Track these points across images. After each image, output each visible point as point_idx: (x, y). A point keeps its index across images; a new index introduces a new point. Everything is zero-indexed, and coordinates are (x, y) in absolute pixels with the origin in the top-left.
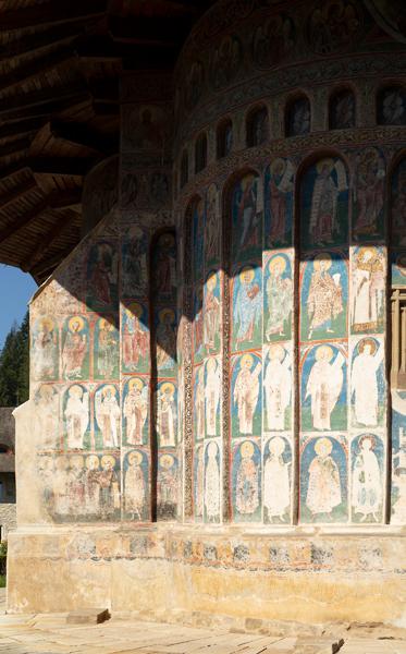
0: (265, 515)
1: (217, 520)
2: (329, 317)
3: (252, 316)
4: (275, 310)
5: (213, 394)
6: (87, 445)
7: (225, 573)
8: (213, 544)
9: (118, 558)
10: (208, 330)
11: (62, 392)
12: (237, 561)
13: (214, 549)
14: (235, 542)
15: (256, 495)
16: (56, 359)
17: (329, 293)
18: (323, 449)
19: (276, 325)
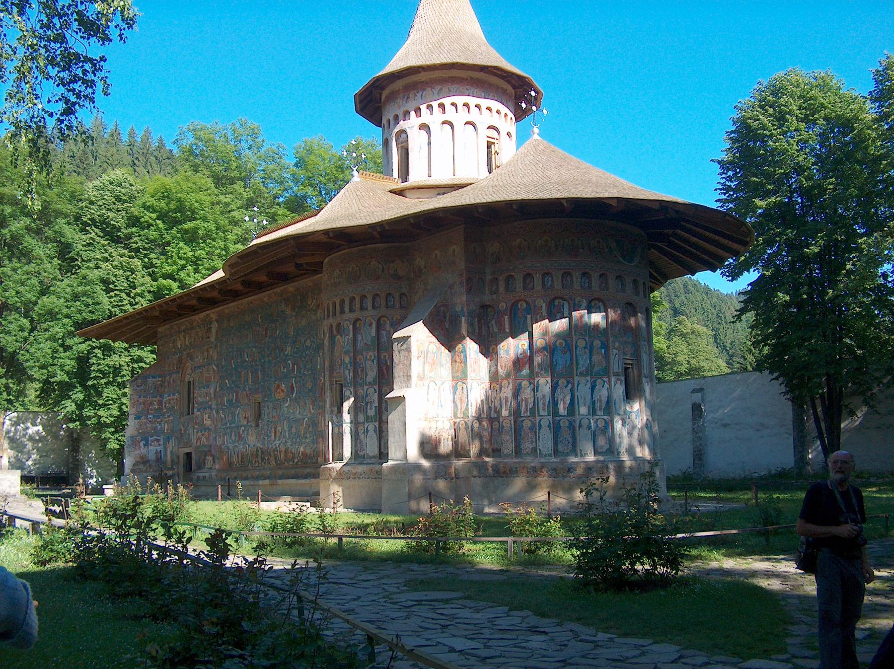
0: (581, 453)
1: (550, 455)
4: (581, 362)
9: (475, 477)
11: (426, 385)
15: (570, 444)
16: (423, 367)
19: (582, 369)
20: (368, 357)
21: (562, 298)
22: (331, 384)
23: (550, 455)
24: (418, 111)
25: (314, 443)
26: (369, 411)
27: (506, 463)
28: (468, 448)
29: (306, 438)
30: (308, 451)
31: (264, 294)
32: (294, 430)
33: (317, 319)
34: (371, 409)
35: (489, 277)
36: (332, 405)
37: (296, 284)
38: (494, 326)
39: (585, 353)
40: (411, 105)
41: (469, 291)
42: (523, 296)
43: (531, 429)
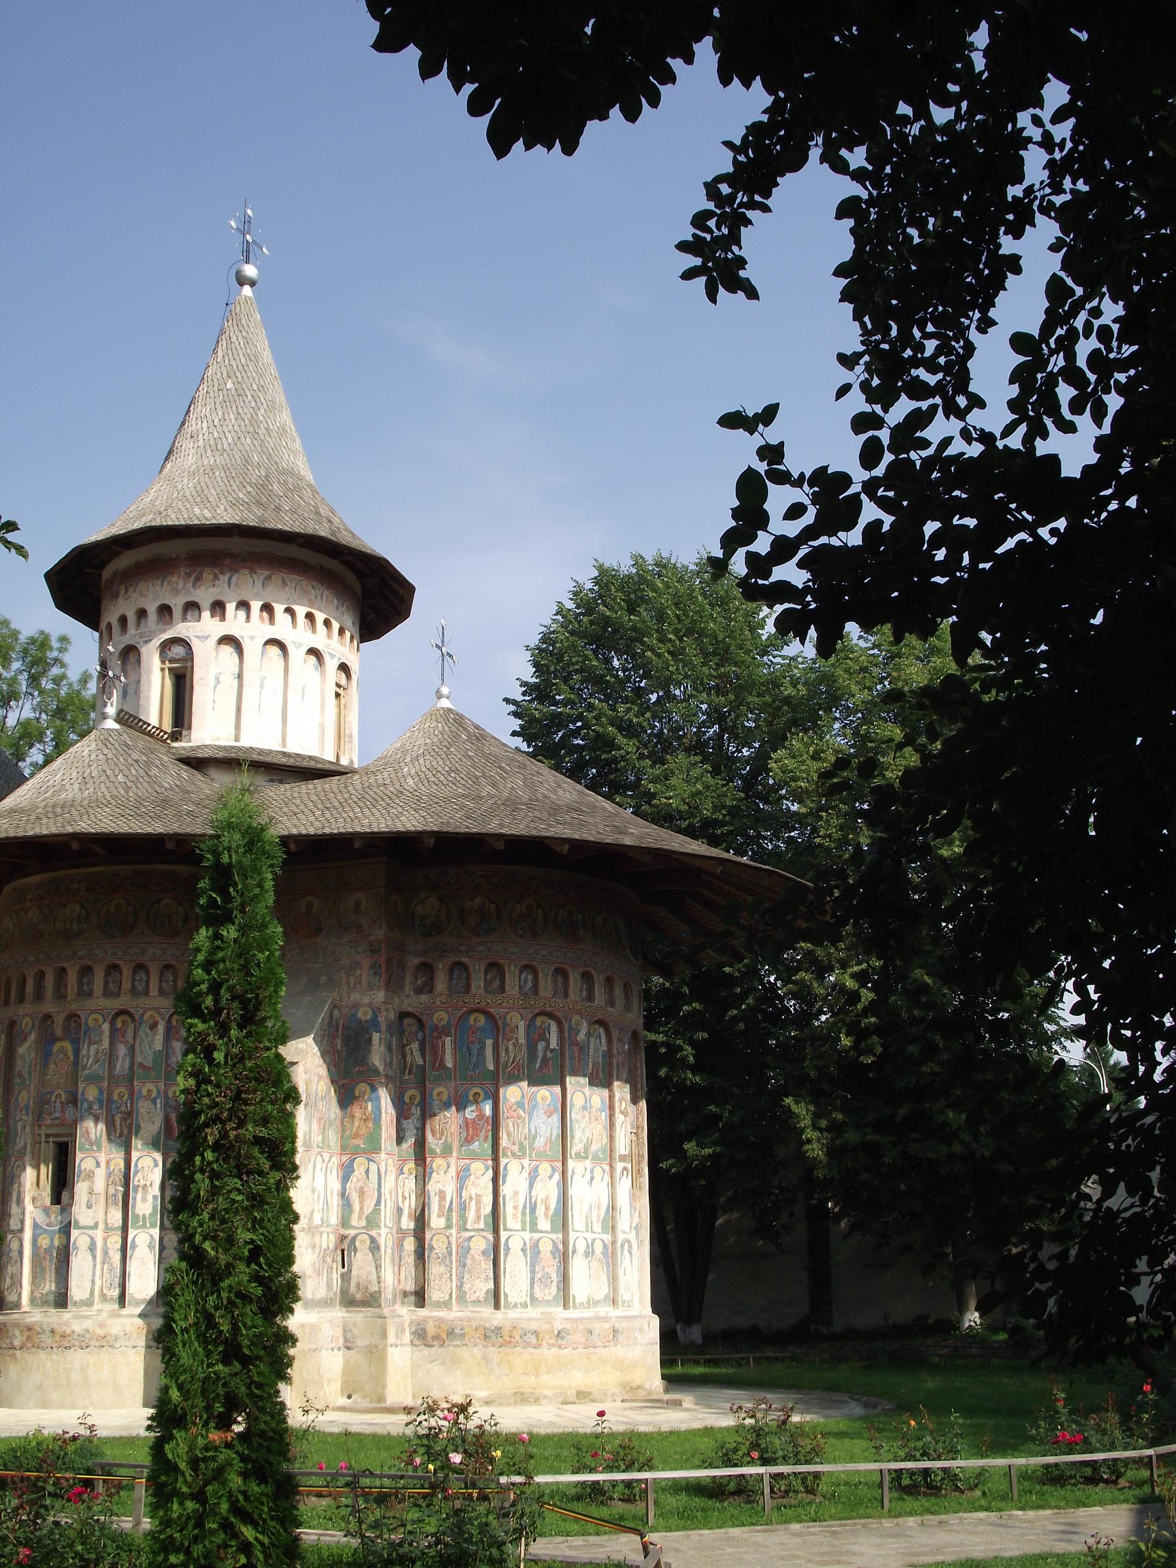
0: (574, 1301)
1: (524, 1305)
2: (600, 1145)
3: (549, 1132)
4: (578, 1134)
5: (516, 1193)
6: (322, 1219)
7: (547, 1353)
8: (533, 1326)
11: (312, 1161)
12: (560, 1342)
13: (536, 1333)
14: (558, 1326)
15: (555, 1284)
17: (600, 1127)
18: (599, 1247)
20: (144, 1093)
21: (550, 1015)
22: (36, 1142)
23: (524, 1305)
24: (218, 608)
27: (440, 1320)
28: (374, 1288)
34: (144, 1200)
35: (416, 961)
38: (417, 1054)
39: (584, 1117)
40: (205, 595)
41: (389, 982)
43: (484, 1253)
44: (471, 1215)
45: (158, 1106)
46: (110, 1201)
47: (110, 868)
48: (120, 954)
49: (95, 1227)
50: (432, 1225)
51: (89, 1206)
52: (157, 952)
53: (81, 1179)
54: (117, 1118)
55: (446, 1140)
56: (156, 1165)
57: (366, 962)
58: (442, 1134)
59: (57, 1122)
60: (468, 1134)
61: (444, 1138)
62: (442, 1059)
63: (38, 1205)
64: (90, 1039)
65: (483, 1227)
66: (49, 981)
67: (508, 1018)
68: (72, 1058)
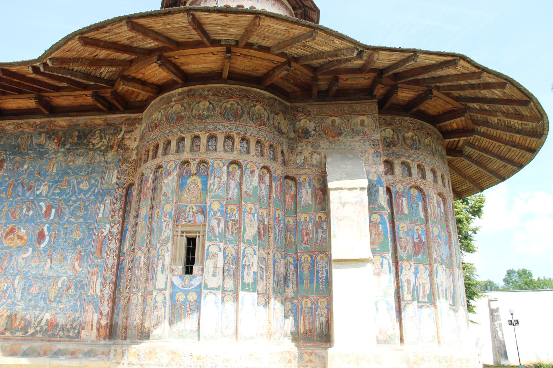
5: (442, 283)
10: (436, 252)
20: (248, 209)
25: (76, 311)
26: (246, 276)
29: (60, 302)
30: (61, 320)
31: (7, 122)
32: (35, 289)
33: (106, 161)
34: (249, 274)
36: (173, 261)
37: (74, 119)
42: (418, 183)
44: (421, 294)
45: (256, 218)
46: (225, 274)
47: (227, 85)
48: (234, 129)
49: (218, 289)
50: (405, 298)
51: (214, 276)
52: (254, 132)
53: (209, 258)
54: (230, 224)
55: (408, 252)
56: (255, 254)
57: (371, 150)
58: (406, 248)
59: (190, 224)
60: (416, 250)
61: (407, 251)
62: (402, 209)
63: (176, 273)
64: (215, 175)
65: (427, 301)
66: (188, 142)
67: (429, 192)
68: (200, 187)
